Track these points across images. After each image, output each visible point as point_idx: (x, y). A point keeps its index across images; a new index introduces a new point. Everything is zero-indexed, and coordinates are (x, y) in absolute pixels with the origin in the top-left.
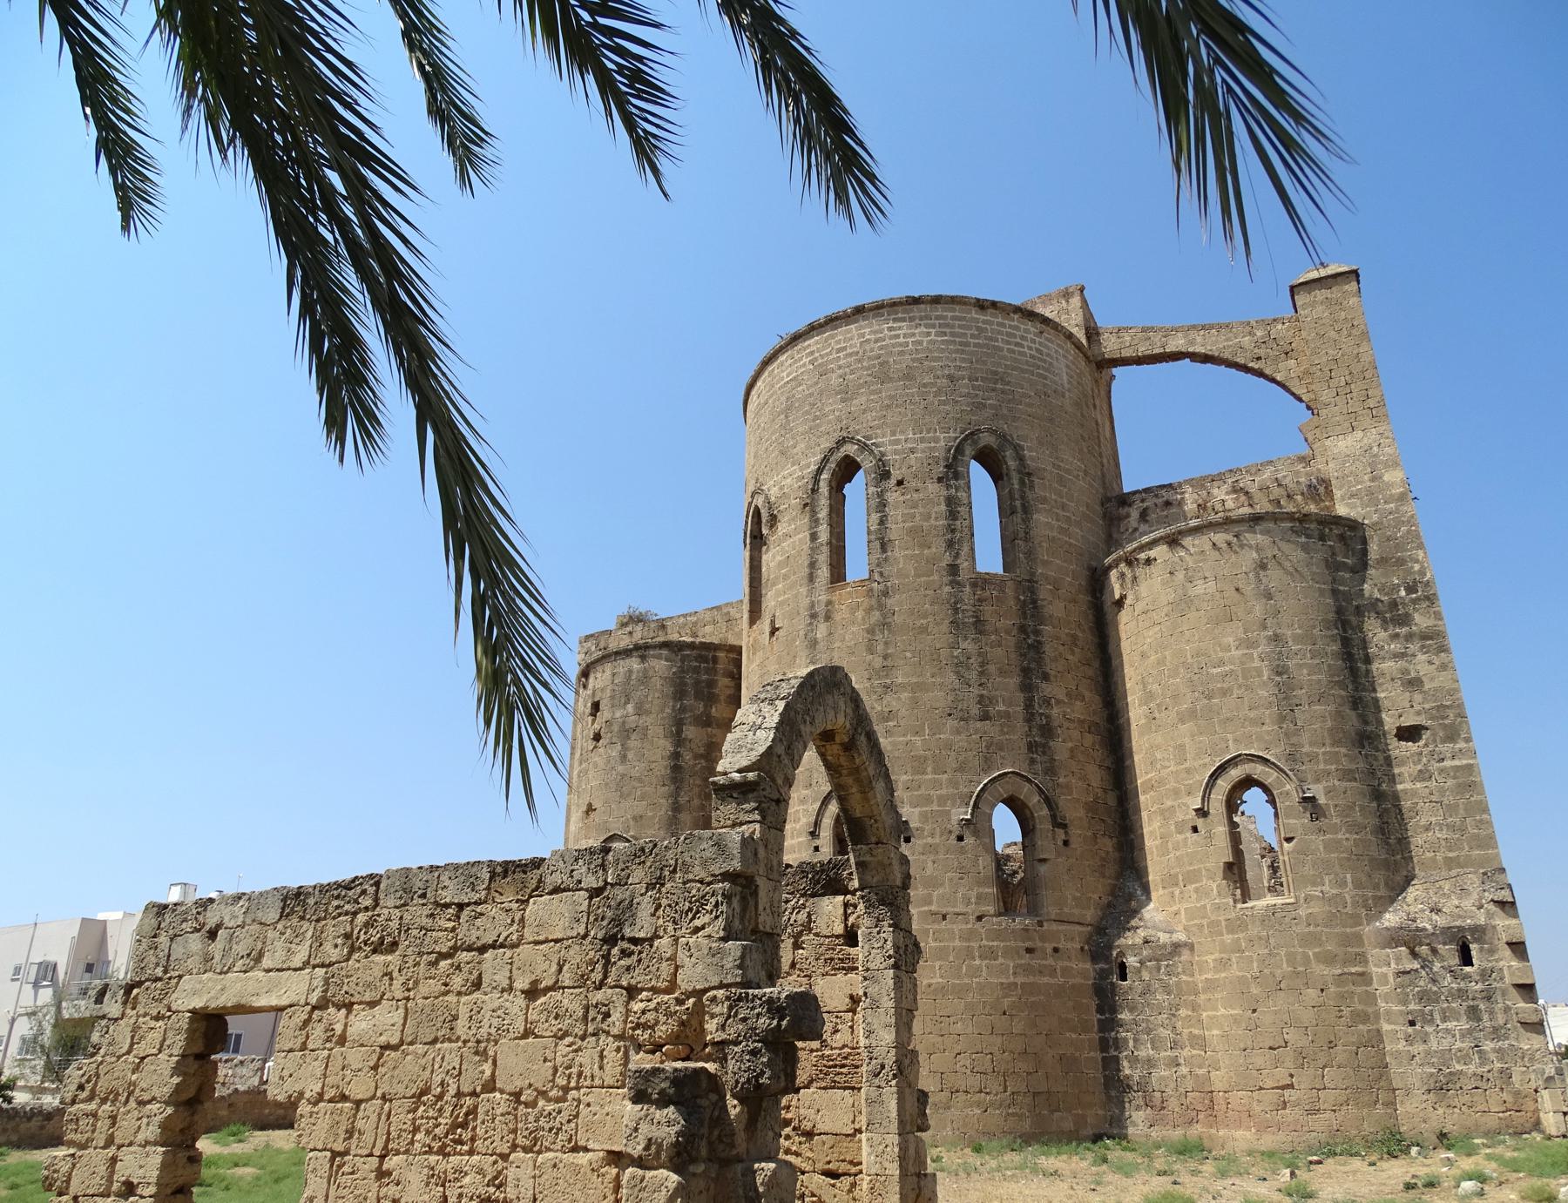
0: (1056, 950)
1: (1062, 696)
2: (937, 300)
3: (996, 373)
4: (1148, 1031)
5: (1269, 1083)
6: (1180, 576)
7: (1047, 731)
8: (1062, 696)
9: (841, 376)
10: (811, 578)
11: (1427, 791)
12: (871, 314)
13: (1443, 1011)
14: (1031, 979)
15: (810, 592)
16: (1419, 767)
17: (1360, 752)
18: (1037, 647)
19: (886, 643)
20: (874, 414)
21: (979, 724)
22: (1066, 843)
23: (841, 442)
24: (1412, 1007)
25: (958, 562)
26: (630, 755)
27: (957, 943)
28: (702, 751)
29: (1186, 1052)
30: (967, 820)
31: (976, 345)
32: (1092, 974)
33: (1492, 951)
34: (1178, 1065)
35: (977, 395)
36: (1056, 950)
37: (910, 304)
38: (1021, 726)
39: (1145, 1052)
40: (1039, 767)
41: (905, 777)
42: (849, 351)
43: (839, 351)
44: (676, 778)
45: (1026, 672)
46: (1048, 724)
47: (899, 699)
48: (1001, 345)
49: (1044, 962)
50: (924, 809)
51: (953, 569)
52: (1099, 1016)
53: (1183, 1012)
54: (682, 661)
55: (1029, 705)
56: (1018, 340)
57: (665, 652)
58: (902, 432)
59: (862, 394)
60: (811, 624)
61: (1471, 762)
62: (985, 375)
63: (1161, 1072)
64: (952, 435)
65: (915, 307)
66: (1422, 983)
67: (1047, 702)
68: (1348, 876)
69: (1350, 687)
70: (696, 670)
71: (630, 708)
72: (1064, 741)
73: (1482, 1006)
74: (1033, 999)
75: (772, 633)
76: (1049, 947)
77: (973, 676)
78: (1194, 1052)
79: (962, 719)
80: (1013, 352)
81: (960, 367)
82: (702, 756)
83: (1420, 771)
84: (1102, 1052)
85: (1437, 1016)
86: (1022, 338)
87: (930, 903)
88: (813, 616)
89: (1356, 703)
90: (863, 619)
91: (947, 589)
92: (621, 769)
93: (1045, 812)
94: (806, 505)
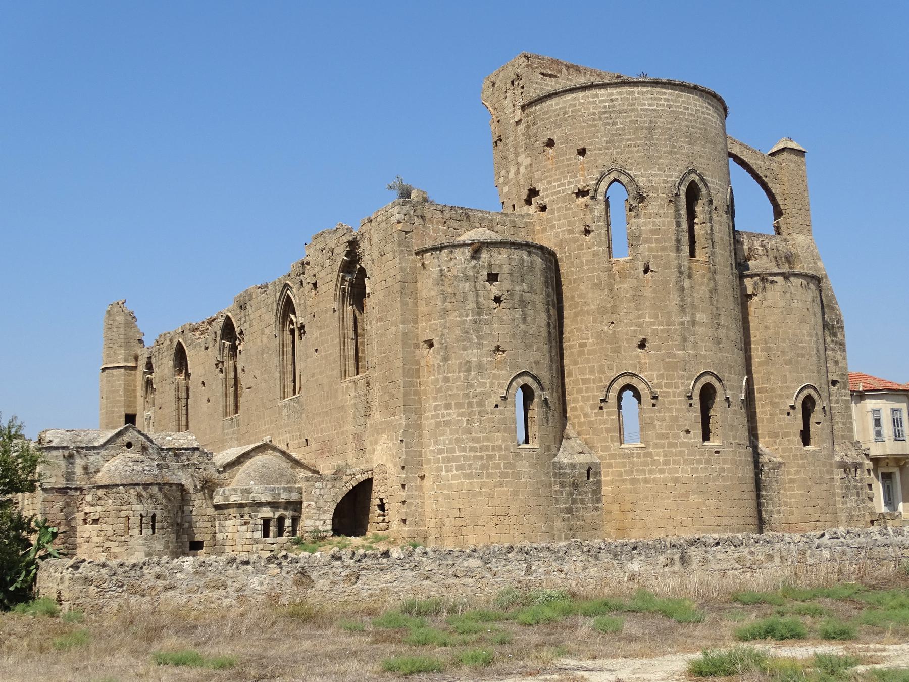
10: (678, 249)
12: (699, 93)
23: (691, 171)
43: (685, 108)
75: (646, 272)
88: (681, 273)
94: (671, 201)
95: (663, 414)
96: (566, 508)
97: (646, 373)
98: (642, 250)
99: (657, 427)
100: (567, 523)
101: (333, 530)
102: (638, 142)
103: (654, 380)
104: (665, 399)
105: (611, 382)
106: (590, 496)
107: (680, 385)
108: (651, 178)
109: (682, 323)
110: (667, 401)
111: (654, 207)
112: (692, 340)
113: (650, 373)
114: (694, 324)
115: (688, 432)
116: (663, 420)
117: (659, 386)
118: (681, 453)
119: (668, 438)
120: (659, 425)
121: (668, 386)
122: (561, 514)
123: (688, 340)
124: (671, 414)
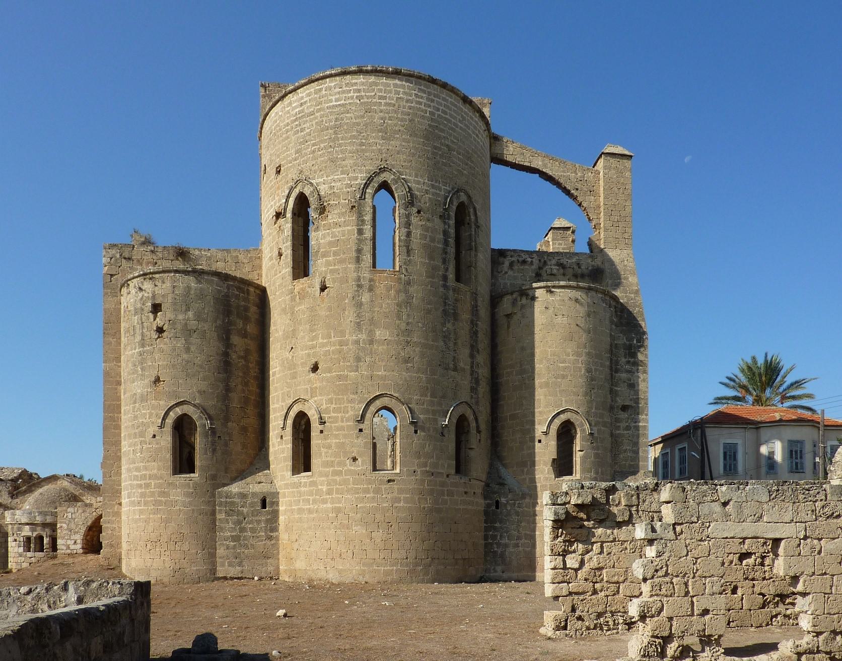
6: (551, 310)
9: (382, 119)
10: (358, 260)
11: (628, 435)
15: (358, 270)
18: (476, 333)
19: (408, 315)
23: (382, 170)
28: (242, 354)
29: (523, 541)
30: (446, 425)
34: (518, 547)
36: (474, 493)
37: (429, 82)
38: (469, 377)
39: (505, 541)
41: (415, 397)
45: (472, 347)
46: (478, 378)
47: (414, 351)
50: (425, 416)
52: (485, 525)
53: (523, 524)
57: (215, 279)
58: (422, 177)
59: (397, 138)
61: (645, 424)
63: (511, 549)
70: (237, 297)
71: (190, 314)
76: (473, 491)
77: (451, 344)
78: (526, 541)
82: (242, 357)
83: (627, 426)
84: (485, 541)
87: (426, 466)
88: (360, 286)
90: (395, 296)
91: (441, 289)
92: (185, 356)
94: (353, 207)
95: (329, 441)
96: (232, 536)
97: (316, 398)
98: (320, 265)
99: (323, 454)
100: (232, 550)
101: (83, 548)
102: (322, 145)
103: (322, 405)
104: (333, 425)
105: (288, 410)
107: (349, 409)
108: (333, 184)
109: (357, 342)
110: (335, 427)
111: (334, 216)
112: (368, 359)
113: (320, 397)
114: (371, 342)
115: (355, 459)
116: (329, 447)
117: (327, 411)
118: (345, 482)
119: (332, 466)
120: (326, 453)
121: (335, 410)
123: (363, 360)
124: (338, 441)
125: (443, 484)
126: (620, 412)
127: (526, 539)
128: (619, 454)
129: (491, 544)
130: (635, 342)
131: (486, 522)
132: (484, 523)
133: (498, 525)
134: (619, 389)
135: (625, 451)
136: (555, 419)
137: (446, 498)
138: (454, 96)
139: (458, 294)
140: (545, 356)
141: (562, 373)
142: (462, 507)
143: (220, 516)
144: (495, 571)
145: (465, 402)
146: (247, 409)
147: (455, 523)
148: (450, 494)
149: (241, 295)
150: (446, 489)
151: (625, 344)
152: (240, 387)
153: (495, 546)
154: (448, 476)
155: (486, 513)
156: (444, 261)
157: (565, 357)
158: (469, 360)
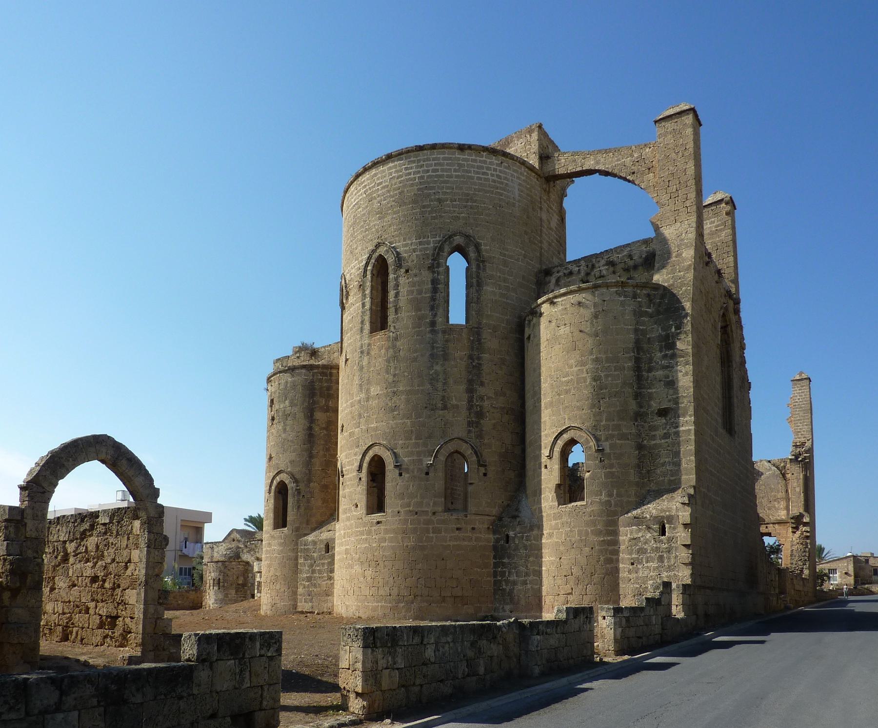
0: (473, 529)
1: (491, 395)
2: (434, 147)
3: (468, 195)
4: (515, 568)
5: (563, 592)
7: (480, 415)
8: (491, 395)
12: (397, 158)
13: (647, 558)
14: (458, 543)
16: (665, 431)
17: (634, 424)
18: (479, 367)
20: (395, 227)
21: (441, 412)
22: (485, 475)
23: (378, 246)
24: (633, 556)
25: (436, 319)
26: (288, 428)
27: (422, 526)
29: (531, 578)
30: (431, 464)
31: (457, 176)
32: (493, 540)
33: (674, 528)
34: (526, 584)
35: (454, 211)
38: (464, 412)
39: (513, 578)
40: (473, 435)
41: (401, 442)
42: (384, 184)
43: (379, 184)
44: (310, 440)
45: (470, 382)
46: (481, 410)
47: (400, 399)
48: (473, 175)
49: (466, 535)
50: (410, 458)
51: (433, 324)
52: (494, 560)
53: (531, 559)
54: (313, 376)
55: (470, 400)
56: (485, 170)
57: (304, 371)
58: (409, 239)
60: (361, 357)
62: (460, 197)
63: (519, 587)
64: (438, 239)
65: (421, 153)
66: (640, 544)
67: (482, 398)
68: (615, 491)
69: (635, 386)
71: (287, 402)
72: (490, 420)
73: (665, 555)
74: (459, 552)
76: (469, 527)
77: (439, 385)
78: (534, 578)
79: (432, 410)
80: (480, 179)
81: (446, 192)
82: (324, 428)
84: (494, 578)
85: (644, 560)
86: (488, 169)
87: (409, 506)
89: (637, 396)
90: (385, 354)
91: (429, 335)
92: (283, 436)
93: (474, 458)
94: (361, 285)
100: (306, 589)
106: (326, 567)
114: (368, 399)
122: (303, 582)
125: (428, 522)
126: (656, 418)
127: (534, 576)
128: (655, 469)
129: (500, 581)
130: (673, 330)
131: (495, 558)
132: (493, 559)
133: (506, 560)
134: (654, 390)
135: (663, 464)
136: (557, 440)
137: (431, 535)
138: (446, 151)
139: (449, 334)
140: (550, 373)
141: (565, 388)
142: (451, 543)
143: (301, 561)
144: (504, 611)
145: (457, 438)
146: (328, 470)
147: (443, 559)
148: (437, 531)
149: (324, 378)
150: (431, 526)
151: (660, 335)
152: (321, 453)
153: (504, 583)
154: (434, 513)
155: (495, 548)
156: (432, 308)
157: (567, 370)
158: (465, 396)
